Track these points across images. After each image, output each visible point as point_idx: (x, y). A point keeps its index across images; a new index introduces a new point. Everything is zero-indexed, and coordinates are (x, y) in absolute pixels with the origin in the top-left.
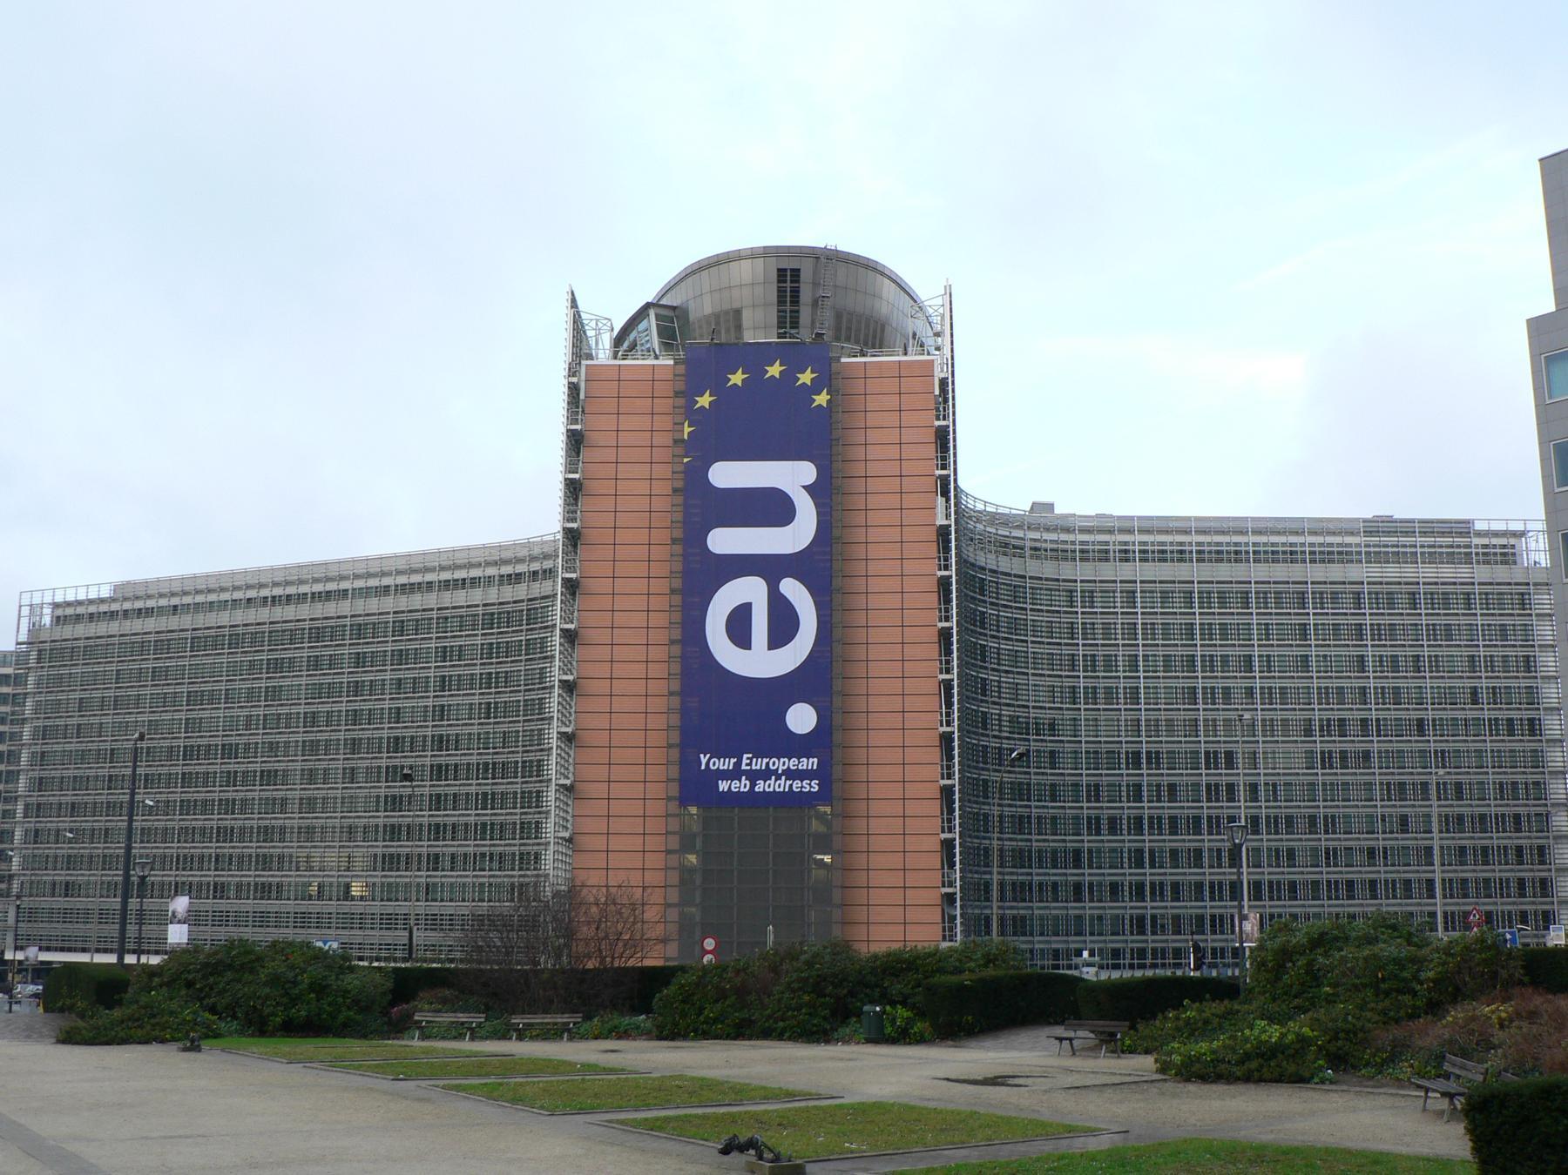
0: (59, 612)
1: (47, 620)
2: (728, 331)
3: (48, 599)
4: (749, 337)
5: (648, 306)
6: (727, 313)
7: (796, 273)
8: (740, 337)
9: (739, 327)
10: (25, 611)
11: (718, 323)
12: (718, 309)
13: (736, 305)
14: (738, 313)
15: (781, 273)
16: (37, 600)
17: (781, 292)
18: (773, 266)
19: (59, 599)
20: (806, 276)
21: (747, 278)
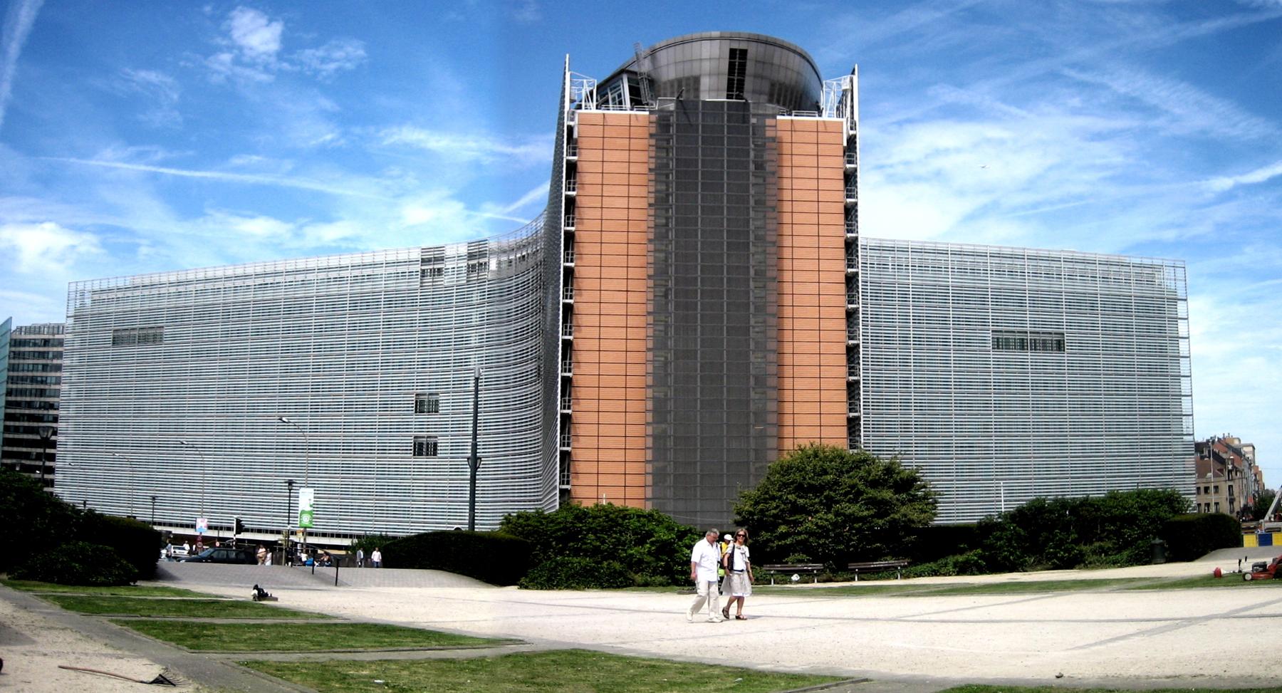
0: (96, 297)
1: (88, 301)
2: (688, 91)
3: (89, 287)
4: (706, 97)
5: (622, 71)
6: (688, 79)
7: (744, 53)
8: (698, 96)
9: (697, 90)
10: (73, 296)
11: (680, 86)
12: (680, 75)
13: (696, 73)
14: (697, 80)
15: (733, 52)
16: (80, 287)
17: (731, 66)
18: (727, 47)
19: (96, 288)
20: (749, 56)
21: (706, 55)
